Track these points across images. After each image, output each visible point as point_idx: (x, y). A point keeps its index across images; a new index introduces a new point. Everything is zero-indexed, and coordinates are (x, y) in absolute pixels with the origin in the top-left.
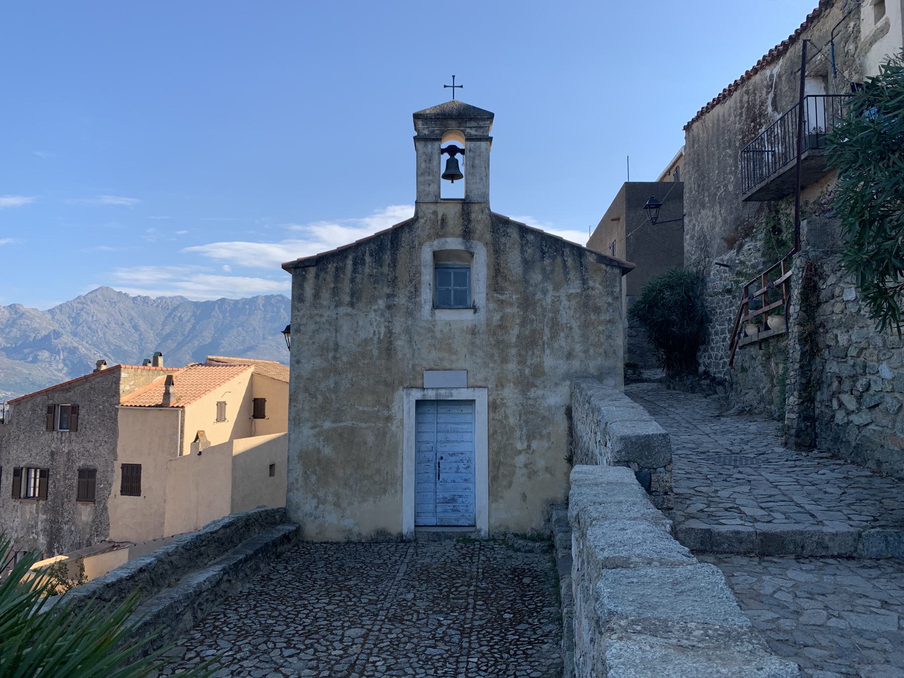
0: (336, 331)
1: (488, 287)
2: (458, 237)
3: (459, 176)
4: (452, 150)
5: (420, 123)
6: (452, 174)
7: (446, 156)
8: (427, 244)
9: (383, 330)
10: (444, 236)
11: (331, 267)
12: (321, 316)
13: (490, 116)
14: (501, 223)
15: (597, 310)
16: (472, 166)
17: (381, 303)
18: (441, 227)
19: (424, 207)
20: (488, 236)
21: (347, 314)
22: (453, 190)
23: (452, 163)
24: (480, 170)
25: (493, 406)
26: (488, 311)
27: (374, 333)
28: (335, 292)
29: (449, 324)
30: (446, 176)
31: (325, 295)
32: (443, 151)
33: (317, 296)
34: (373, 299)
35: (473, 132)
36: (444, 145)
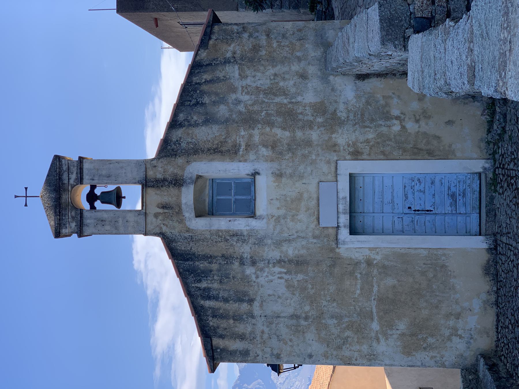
0: (279, 317)
1: (232, 160)
2: (180, 192)
3: (118, 191)
4: (92, 198)
5: (64, 231)
6: (117, 198)
7: (98, 204)
8: (188, 223)
9: (277, 269)
11: (212, 322)
12: (263, 332)
13: (57, 159)
15: (256, 48)
16: (108, 178)
17: (249, 271)
18: (170, 209)
19: (150, 227)
20: (180, 161)
21: (261, 306)
22: (133, 198)
23: (106, 198)
24: (111, 169)
25: (356, 155)
26: (257, 159)
27: (281, 278)
28: (238, 318)
30: (119, 205)
31: (241, 328)
32: (93, 207)
33: (242, 337)
34: (245, 279)
35: (73, 176)
36: (86, 206)
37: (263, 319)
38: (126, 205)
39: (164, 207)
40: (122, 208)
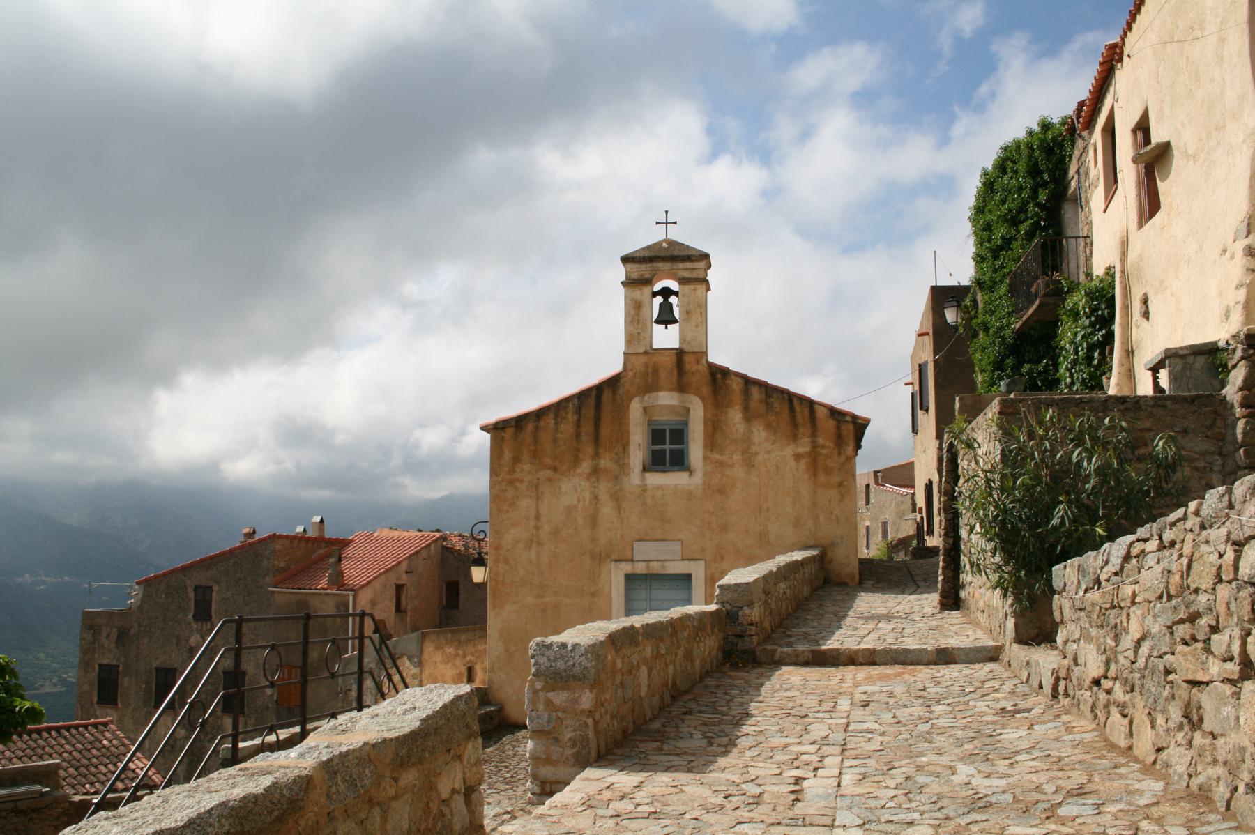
1: (705, 446)
3: (675, 321)
4: (666, 293)
5: (629, 265)
6: (666, 318)
7: (659, 300)
8: (636, 399)
9: (587, 495)
10: (657, 389)
13: (706, 257)
14: (719, 375)
15: (828, 471)
16: (687, 313)
18: (649, 384)
20: (705, 390)
21: (550, 480)
23: (666, 309)
24: (698, 312)
27: (579, 500)
29: (659, 488)
30: (658, 322)
31: (525, 456)
32: (655, 294)
33: (516, 460)
34: (576, 461)
35: (687, 274)
36: (657, 287)
38: (658, 329)
39: (656, 371)
40: (655, 325)
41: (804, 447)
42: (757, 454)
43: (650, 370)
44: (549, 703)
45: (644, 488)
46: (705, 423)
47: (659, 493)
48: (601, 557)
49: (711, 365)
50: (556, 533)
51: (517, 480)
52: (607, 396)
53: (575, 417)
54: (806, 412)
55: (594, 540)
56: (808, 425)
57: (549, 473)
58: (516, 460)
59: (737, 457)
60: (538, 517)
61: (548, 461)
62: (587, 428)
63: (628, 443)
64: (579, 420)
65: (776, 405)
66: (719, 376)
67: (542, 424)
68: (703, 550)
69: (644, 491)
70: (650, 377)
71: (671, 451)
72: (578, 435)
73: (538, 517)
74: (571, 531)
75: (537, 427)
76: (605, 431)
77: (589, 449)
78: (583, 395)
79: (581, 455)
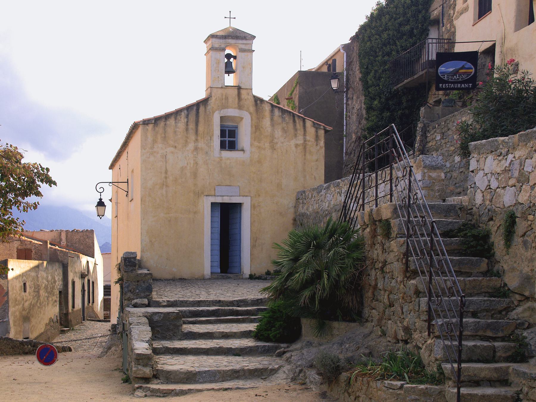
0: (166, 162)
1: (251, 138)
2: (235, 108)
3: (233, 72)
4: (229, 56)
6: (229, 70)
8: (217, 112)
9: (192, 162)
11: (162, 124)
12: (158, 153)
17: (191, 146)
19: (215, 90)
20: (252, 109)
21: (172, 153)
22: (230, 80)
23: (228, 65)
25: (253, 207)
26: (251, 153)
27: (187, 164)
28: (165, 138)
29: (228, 159)
31: (159, 139)
33: (155, 141)
34: (186, 143)
35: (243, 47)
37: (165, 154)
39: (227, 98)
41: (300, 141)
42: (277, 143)
43: (224, 97)
44: (430, 177)
45: (221, 159)
46: (252, 127)
47: (228, 162)
48: (199, 194)
49: (254, 97)
50: (176, 180)
51: (155, 152)
52: (202, 109)
53: (186, 120)
54: (301, 123)
55: (195, 185)
56: (302, 130)
57: (172, 149)
58: (155, 141)
59: (267, 145)
60: (166, 172)
61: (171, 142)
62: (192, 126)
63: (213, 135)
64: (187, 122)
65: (287, 119)
66: (258, 102)
67: (168, 122)
68: (250, 192)
69: (221, 160)
70: (224, 101)
71: (229, 141)
72: (187, 130)
73: (166, 172)
74: (183, 180)
75: (165, 124)
76: (201, 128)
77: (193, 137)
78: (189, 108)
79: (188, 141)
